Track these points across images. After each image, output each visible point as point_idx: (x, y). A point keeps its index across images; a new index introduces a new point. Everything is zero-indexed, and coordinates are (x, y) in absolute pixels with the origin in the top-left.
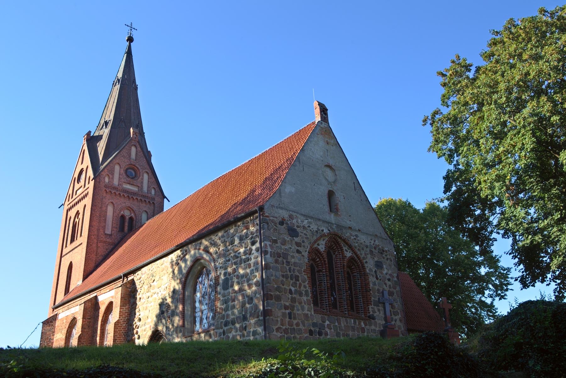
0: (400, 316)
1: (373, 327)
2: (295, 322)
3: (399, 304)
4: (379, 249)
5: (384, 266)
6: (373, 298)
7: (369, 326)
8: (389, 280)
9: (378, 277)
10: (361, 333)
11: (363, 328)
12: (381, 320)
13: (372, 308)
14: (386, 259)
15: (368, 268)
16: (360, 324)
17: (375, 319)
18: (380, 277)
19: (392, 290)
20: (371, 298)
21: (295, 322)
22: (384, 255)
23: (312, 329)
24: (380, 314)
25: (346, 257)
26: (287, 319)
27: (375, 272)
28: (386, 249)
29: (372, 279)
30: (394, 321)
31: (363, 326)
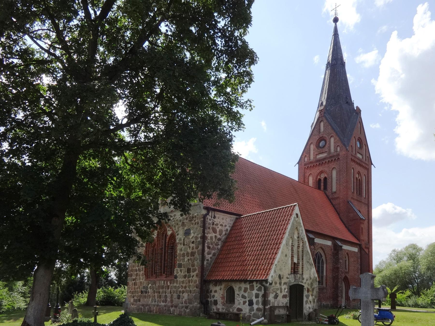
1: (175, 284)
2: (136, 287)
5: (192, 231)
6: (178, 262)
7: (173, 284)
8: (193, 242)
11: (169, 286)
12: (182, 278)
14: (194, 224)
16: (167, 283)
19: (195, 250)
21: (136, 287)
22: (193, 222)
23: (143, 290)
26: (134, 286)
27: (184, 240)
29: (179, 247)
31: (169, 284)
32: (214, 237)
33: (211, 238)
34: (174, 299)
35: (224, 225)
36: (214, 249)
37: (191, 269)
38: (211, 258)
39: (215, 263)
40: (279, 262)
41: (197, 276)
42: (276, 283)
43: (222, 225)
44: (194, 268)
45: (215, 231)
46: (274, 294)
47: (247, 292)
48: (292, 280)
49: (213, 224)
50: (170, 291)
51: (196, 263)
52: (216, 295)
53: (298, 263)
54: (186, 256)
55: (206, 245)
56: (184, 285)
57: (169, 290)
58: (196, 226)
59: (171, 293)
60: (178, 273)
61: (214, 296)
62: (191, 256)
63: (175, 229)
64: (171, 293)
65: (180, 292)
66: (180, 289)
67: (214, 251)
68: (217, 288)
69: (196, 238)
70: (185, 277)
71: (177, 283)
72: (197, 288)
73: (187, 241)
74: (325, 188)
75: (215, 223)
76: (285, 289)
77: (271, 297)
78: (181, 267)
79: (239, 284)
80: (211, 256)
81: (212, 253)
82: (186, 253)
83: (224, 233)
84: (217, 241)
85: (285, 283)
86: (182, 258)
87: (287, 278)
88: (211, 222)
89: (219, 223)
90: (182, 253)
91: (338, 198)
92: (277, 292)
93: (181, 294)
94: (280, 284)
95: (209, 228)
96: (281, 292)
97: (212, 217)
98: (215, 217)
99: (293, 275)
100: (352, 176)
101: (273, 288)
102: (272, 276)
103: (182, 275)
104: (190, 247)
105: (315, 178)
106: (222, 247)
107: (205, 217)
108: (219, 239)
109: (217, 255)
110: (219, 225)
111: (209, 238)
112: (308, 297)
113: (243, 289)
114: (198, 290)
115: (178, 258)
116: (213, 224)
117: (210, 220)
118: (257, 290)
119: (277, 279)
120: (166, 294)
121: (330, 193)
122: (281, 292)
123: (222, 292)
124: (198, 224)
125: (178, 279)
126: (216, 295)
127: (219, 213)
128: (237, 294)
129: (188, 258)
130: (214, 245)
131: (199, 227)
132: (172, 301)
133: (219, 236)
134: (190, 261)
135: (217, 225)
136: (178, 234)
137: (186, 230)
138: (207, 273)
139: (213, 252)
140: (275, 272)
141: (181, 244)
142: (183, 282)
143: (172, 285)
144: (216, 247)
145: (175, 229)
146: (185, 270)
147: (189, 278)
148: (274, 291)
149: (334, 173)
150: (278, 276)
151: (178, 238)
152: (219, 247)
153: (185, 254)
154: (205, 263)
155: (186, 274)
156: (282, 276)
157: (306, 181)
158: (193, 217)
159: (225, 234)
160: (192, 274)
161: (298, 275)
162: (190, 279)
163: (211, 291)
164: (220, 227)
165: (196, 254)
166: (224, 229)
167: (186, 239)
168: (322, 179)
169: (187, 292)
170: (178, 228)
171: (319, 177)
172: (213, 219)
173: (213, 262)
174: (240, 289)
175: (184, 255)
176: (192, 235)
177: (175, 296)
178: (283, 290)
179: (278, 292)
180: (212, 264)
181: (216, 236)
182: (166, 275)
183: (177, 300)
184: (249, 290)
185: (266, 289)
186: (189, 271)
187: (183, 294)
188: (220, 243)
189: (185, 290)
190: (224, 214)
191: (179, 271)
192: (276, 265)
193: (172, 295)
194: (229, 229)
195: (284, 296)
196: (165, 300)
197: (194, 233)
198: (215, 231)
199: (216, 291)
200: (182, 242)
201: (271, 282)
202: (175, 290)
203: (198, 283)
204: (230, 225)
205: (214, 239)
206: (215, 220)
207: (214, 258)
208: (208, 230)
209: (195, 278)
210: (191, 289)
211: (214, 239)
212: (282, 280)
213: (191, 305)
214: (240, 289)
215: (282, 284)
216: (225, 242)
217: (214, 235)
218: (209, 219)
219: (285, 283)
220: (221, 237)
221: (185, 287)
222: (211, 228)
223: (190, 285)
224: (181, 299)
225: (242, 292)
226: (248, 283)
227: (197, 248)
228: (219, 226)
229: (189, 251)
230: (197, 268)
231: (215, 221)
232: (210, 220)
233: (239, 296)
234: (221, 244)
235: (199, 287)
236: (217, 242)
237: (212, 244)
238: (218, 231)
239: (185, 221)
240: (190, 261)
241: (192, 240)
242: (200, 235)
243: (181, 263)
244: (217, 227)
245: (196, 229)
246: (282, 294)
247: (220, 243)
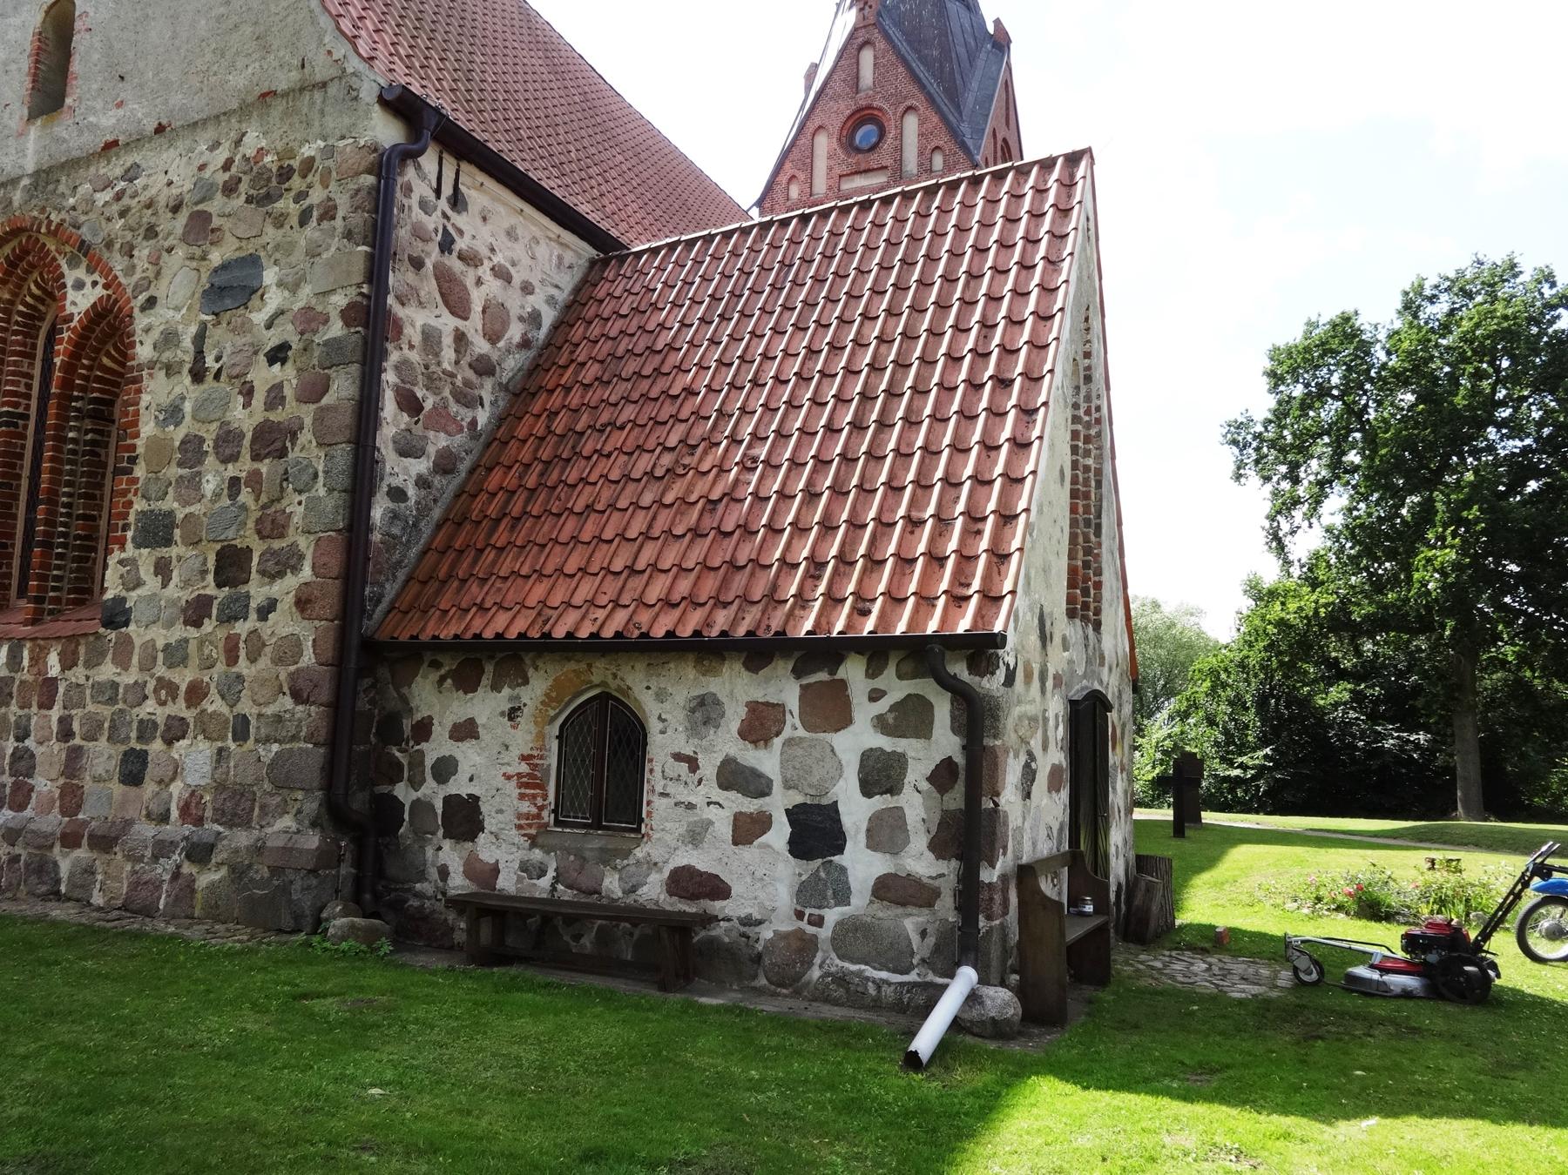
0: (307, 573)
1: (107, 671)
3: (322, 492)
4: (261, 177)
5: (270, 276)
6: (139, 505)
8: (278, 355)
9: (210, 361)
10: (34, 709)
13: (121, 562)
14: (294, 221)
15: (155, 334)
16: (38, 660)
17: (126, 624)
18: (218, 359)
19: (292, 409)
20: (130, 504)
22: (286, 204)
24: (164, 586)
25: (70, 318)
27: (200, 339)
28: (307, 151)
29: (155, 391)
30: (253, 616)
31: (54, 669)
32: (448, 341)
33: (430, 339)
34: (88, 784)
36: (441, 420)
37: (249, 550)
38: (422, 482)
39: (455, 520)
41: (303, 603)
44: (277, 544)
45: (455, 300)
47: (777, 742)
50: (65, 722)
51: (295, 507)
52: (469, 756)
54: (210, 460)
55: (390, 377)
56: (183, 678)
57: (56, 713)
58: (311, 231)
59: (66, 733)
60: (139, 584)
61: (444, 769)
62: (256, 457)
63: (129, 272)
64: (66, 733)
65: (147, 729)
66: (150, 706)
68: (485, 705)
69: (311, 319)
70: (196, 612)
71: (123, 662)
72: (297, 696)
73: (224, 344)
75: (461, 244)
78: (168, 542)
79: (690, 672)
81: (432, 450)
82: (210, 433)
83: (515, 332)
84: (470, 374)
86: (174, 471)
88: (432, 222)
89: (484, 252)
90: (178, 434)
93: (157, 746)
95: (418, 264)
103: (173, 603)
104: (248, 392)
107: (387, 166)
108: (484, 368)
109: (464, 467)
110: (487, 265)
111: (413, 333)
113: (735, 716)
114: (309, 716)
115: (140, 471)
116: (446, 245)
118: (881, 724)
120: (30, 743)
123: (522, 738)
124: (329, 213)
125: (132, 627)
126: (469, 756)
128: (678, 757)
129: (231, 470)
130: (447, 393)
131: (335, 243)
132: (71, 798)
133: (481, 346)
134: (245, 496)
135: (471, 259)
136: (151, 302)
137: (225, 267)
138: (391, 590)
139: (439, 441)
141: (170, 370)
142: (176, 655)
143: (78, 674)
144: (465, 415)
145: (130, 270)
146: (197, 564)
147: (228, 618)
151: (147, 330)
152: (483, 417)
153: (208, 446)
154: (377, 514)
155: (211, 590)
158: (285, 174)
159: (525, 344)
160: (258, 590)
162: (242, 628)
163: (423, 730)
164: (493, 286)
165: (306, 437)
167: (216, 334)
169: (208, 724)
170: (155, 262)
172: (449, 212)
173: (437, 513)
174: (705, 711)
175: (192, 451)
176: (274, 299)
177: (103, 756)
180: (426, 530)
181: (460, 338)
182: (39, 600)
183: (117, 789)
184: (793, 726)
186: (231, 566)
187: (169, 742)
188: (487, 390)
189: (190, 715)
191: (146, 571)
193: (75, 755)
194: (549, 317)
196: (17, 787)
197: (293, 287)
198: (455, 300)
199: (466, 731)
200: (185, 352)
202: (106, 711)
203: (308, 658)
204: (554, 292)
205: (448, 354)
206: (459, 220)
207: (447, 486)
208: (411, 276)
209: (284, 623)
210: (246, 707)
211: (448, 354)
213: (242, 839)
214: (705, 711)
216: (521, 394)
217: (447, 323)
221: (196, 693)
222: (429, 264)
223: (240, 678)
224: (149, 787)
225: (726, 742)
226: (783, 667)
227: (313, 391)
228: (484, 271)
229: (245, 418)
230: (305, 544)
231: (461, 232)
233: (693, 764)
235: (325, 694)
236: (467, 383)
237: (432, 383)
238: (477, 307)
239: (216, 205)
240: (245, 496)
241: (272, 339)
242: (340, 300)
243: (170, 514)
245: (313, 253)
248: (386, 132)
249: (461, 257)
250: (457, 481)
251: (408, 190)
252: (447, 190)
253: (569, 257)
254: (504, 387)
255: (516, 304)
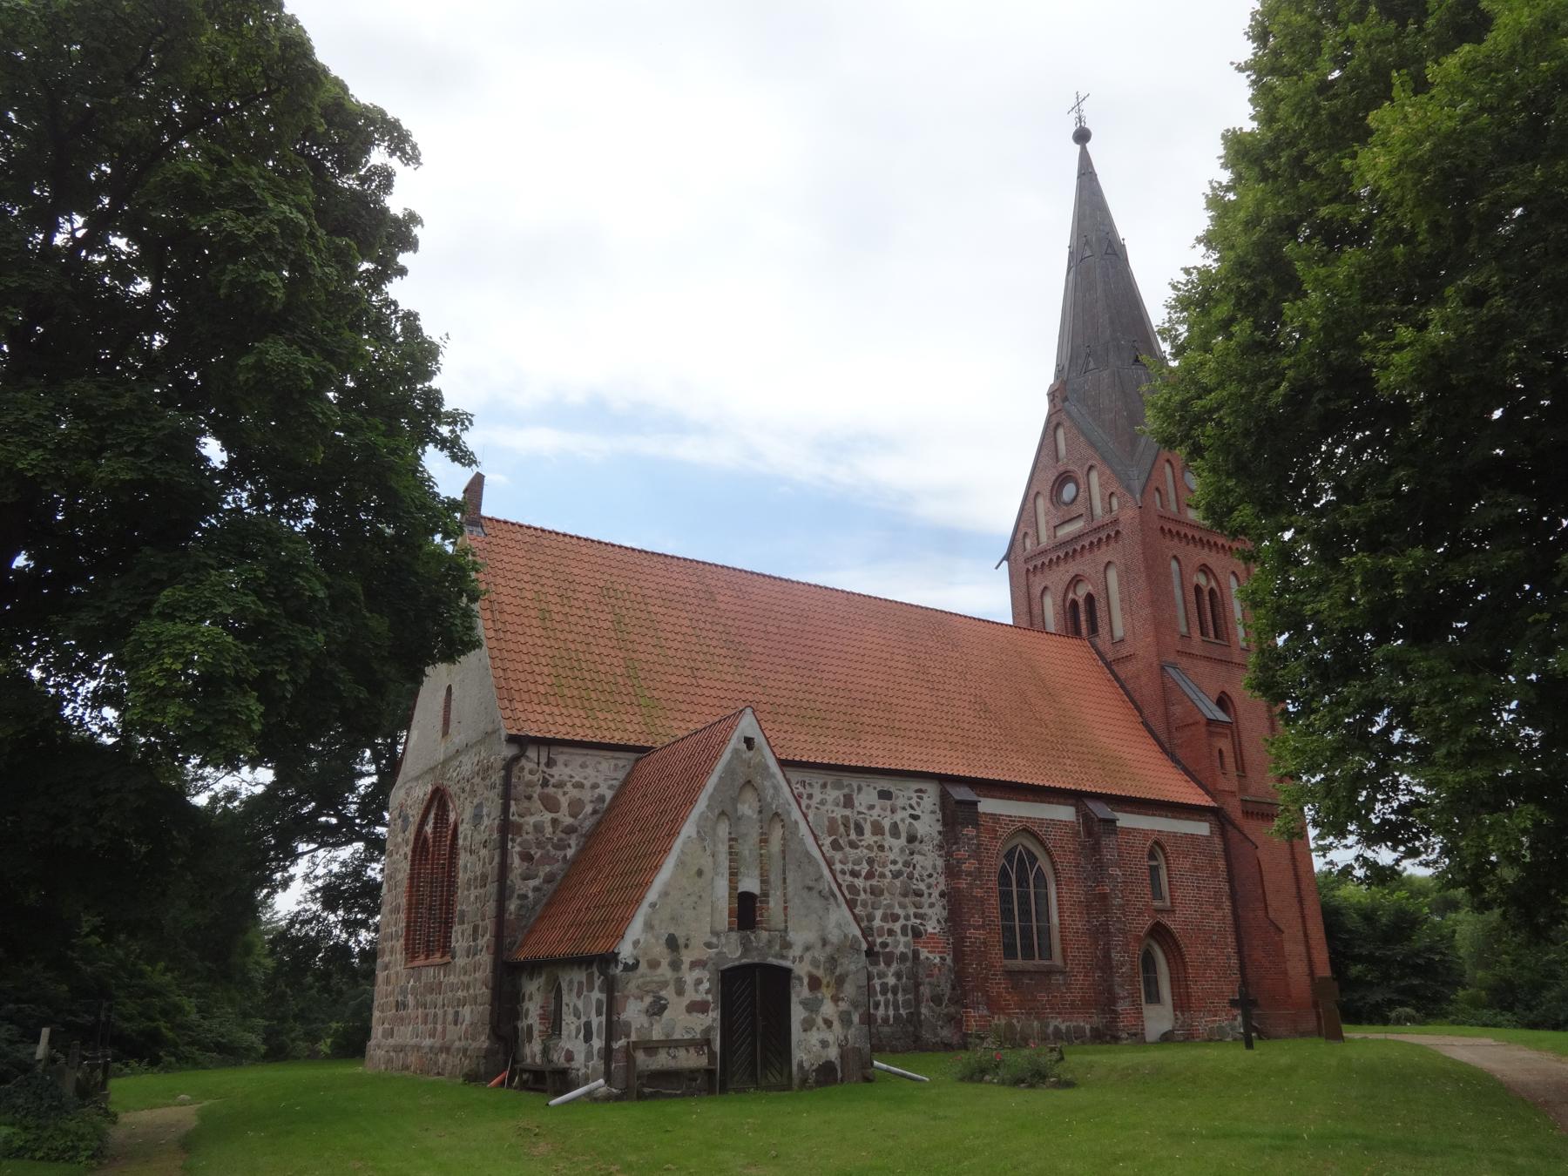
35: (587, 784)
38: (536, 889)
40: (665, 894)
42: (654, 965)
43: (579, 786)
45: (550, 804)
46: (648, 1000)
48: (733, 952)
49: (545, 783)
53: (765, 894)
67: (547, 868)
74: (1093, 629)
75: (552, 781)
76: (699, 982)
77: (633, 1013)
80: (532, 883)
81: (542, 874)
83: (589, 809)
84: (563, 836)
85: (694, 965)
86: (466, 893)
87: (709, 945)
88: (535, 778)
89: (567, 778)
91: (1129, 658)
92: (663, 993)
94: (675, 965)
95: (529, 798)
96: (680, 992)
97: (538, 764)
98: (550, 763)
99: (734, 936)
100: (1176, 581)
101: (641, 980)
102: (636, 943)
105: (1059, 601)
106: (582, 851)
108: (570, 830)
110: (569, 785)
112: (812, 1006)
117: (531, 772)
119: (660, 951)
121: (1108, 644)
122: (680, 992)
127: (566, 750)
130: (549, 847)
133: (568, 820)
135: (560, 785)
140: (649, 926)
144: (560, 854)
148: (648, 992)
149: (1112, 576)
150: (663, 941)
152: (570, 853)
154: (512, 906)
156: (681, 941)
157: (1036, 610)
159: (595, 812)
161: (764, 935)
164: (575, 793)
166: (587, 795)
167: (475, 834)
168: (1081, 602)
171: (1071, 596)
172: (545, 769)
173: (544, 901)
178: (689, 988)
179: (668, 993)
180: (539, 908)
184: (585, 993)
185: (610, 987)
190: (585, 752)
192: (653, 905)
194: (609, 795)
195: (698, 1007)
198: (550, 804)
201: (630, 962)
205: (549, 830)
207: (548, 888)
208: (526, 804)
212: (683, 952)
215: (685, 966)
216: (592, 837)
217: (548, 816)
218: (526, 771)
219: (694, 965)
220: (576, 823)
222: (535, 796)
228: (569, 786)
231: (552, 776)
232: (531, 772)
234: (577, 845)
235: (490, 985)
236: (560, 840)
237: (539, 845)
244: (560, 792)
246: (686, 1001)
247: (573, 842)
248: (508, 752)
249: (554, 786)
250: (554, 885)
251: (522, 769)
252: (543, 760)
253: (621, 763)
254: (584, 835)
255: (587, 795)
